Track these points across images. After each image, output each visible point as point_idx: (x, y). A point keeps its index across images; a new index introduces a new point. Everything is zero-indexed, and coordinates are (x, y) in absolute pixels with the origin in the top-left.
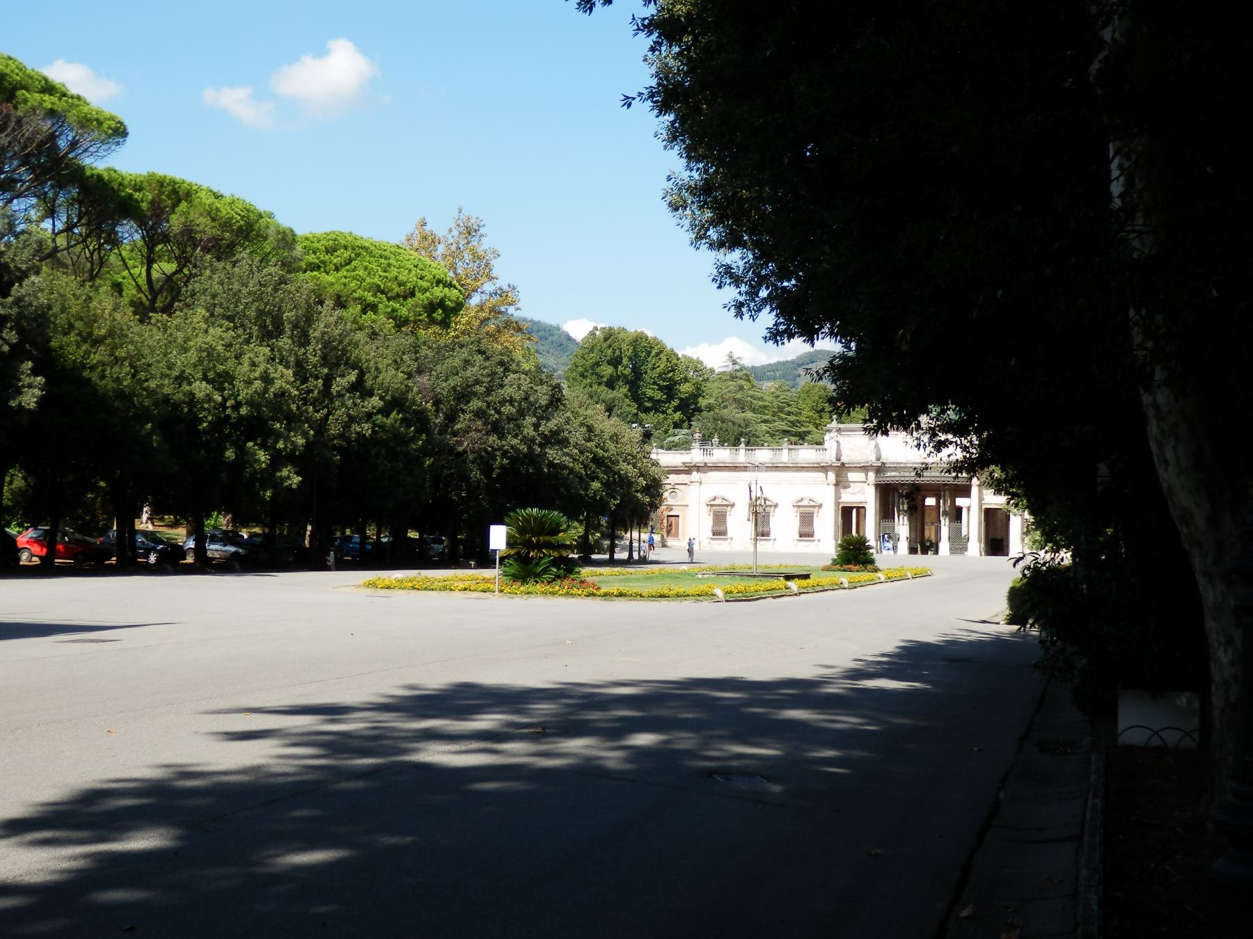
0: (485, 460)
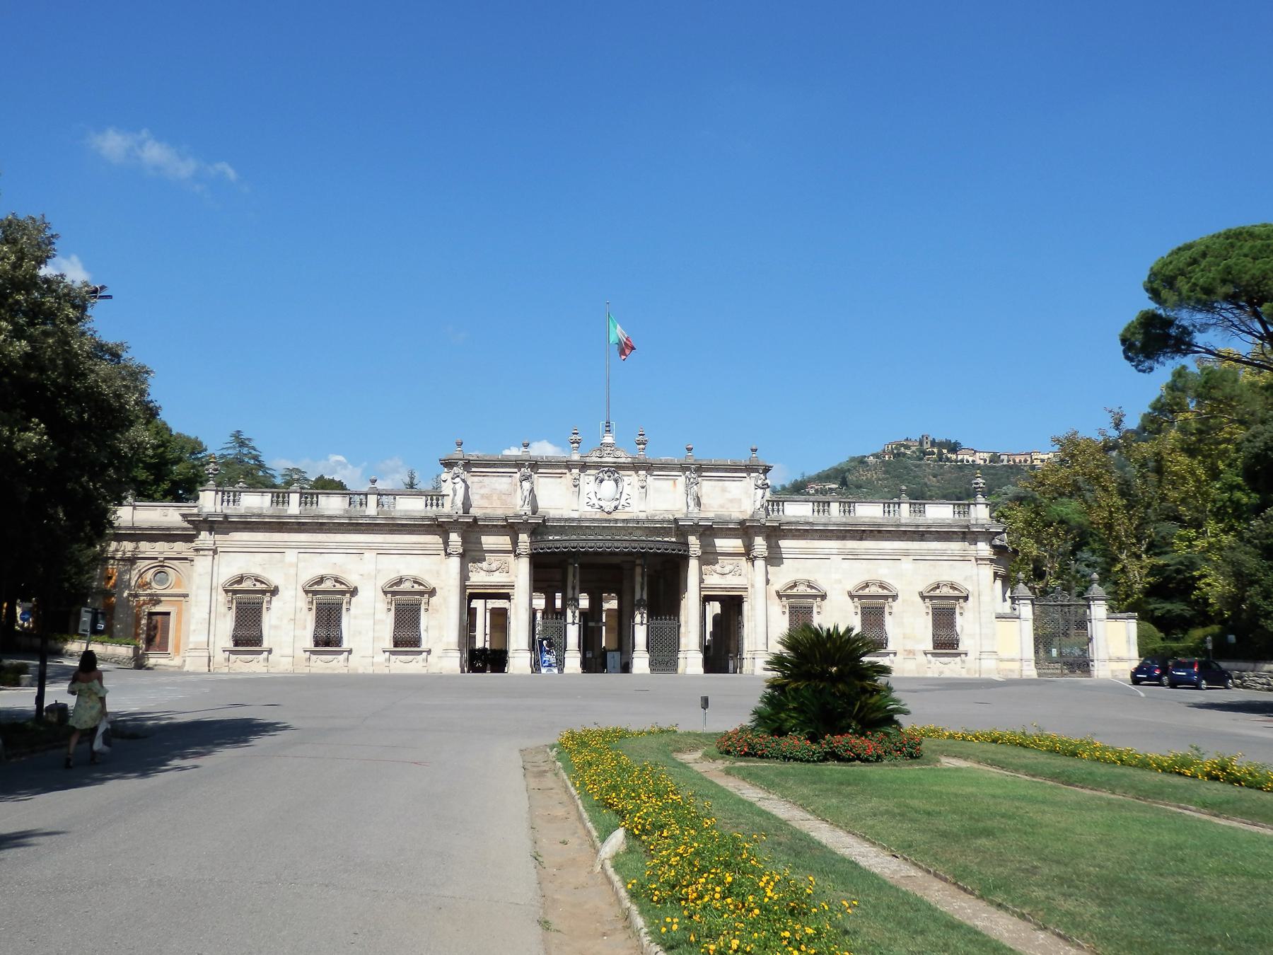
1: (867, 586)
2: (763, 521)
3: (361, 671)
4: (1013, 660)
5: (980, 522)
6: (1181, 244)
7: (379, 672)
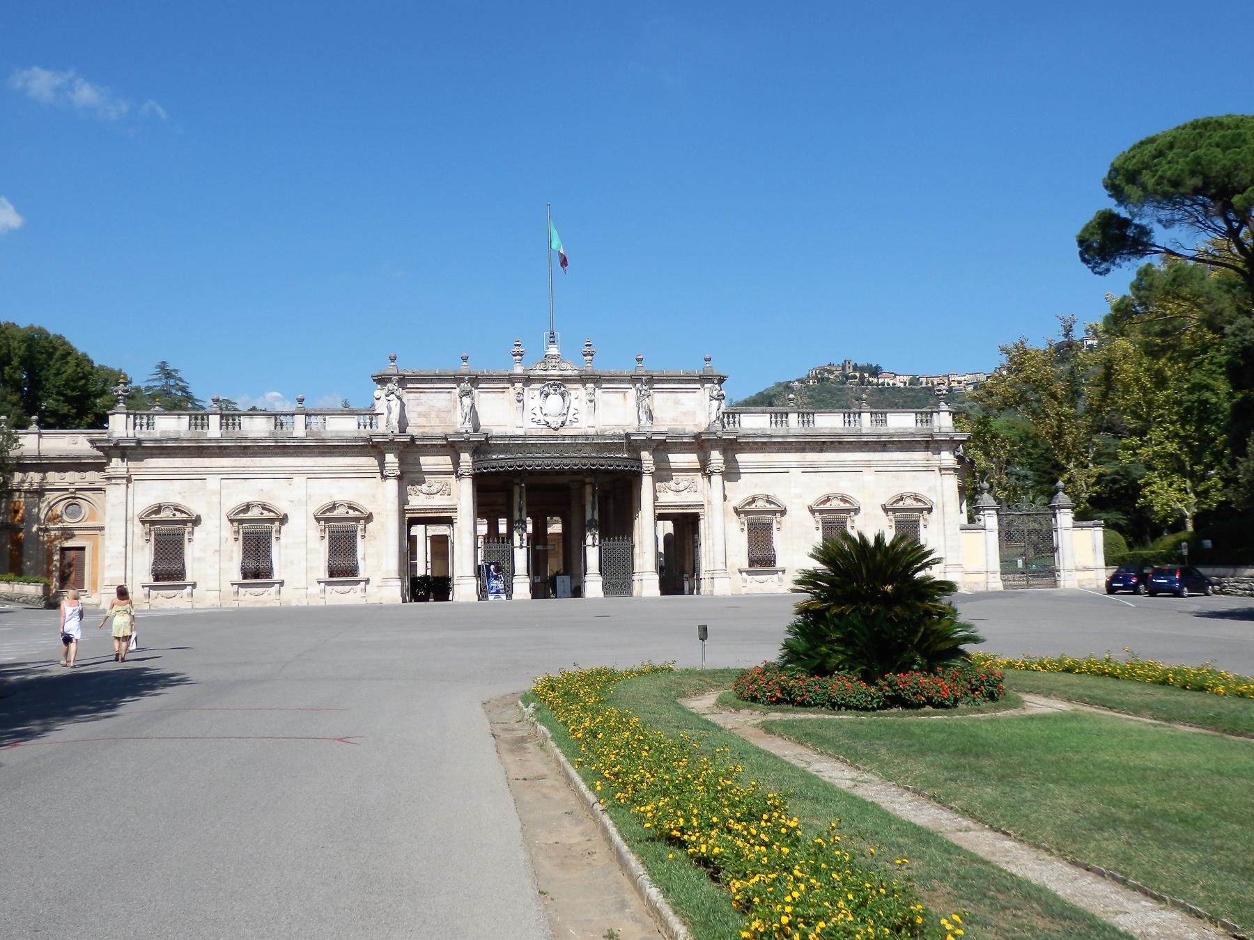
1: (828, 499)
2: (719, 434)
3: (294, 603)
4: (978, 572)
5: (944, 430)
6: (1143, 138)
7: (315, 604)
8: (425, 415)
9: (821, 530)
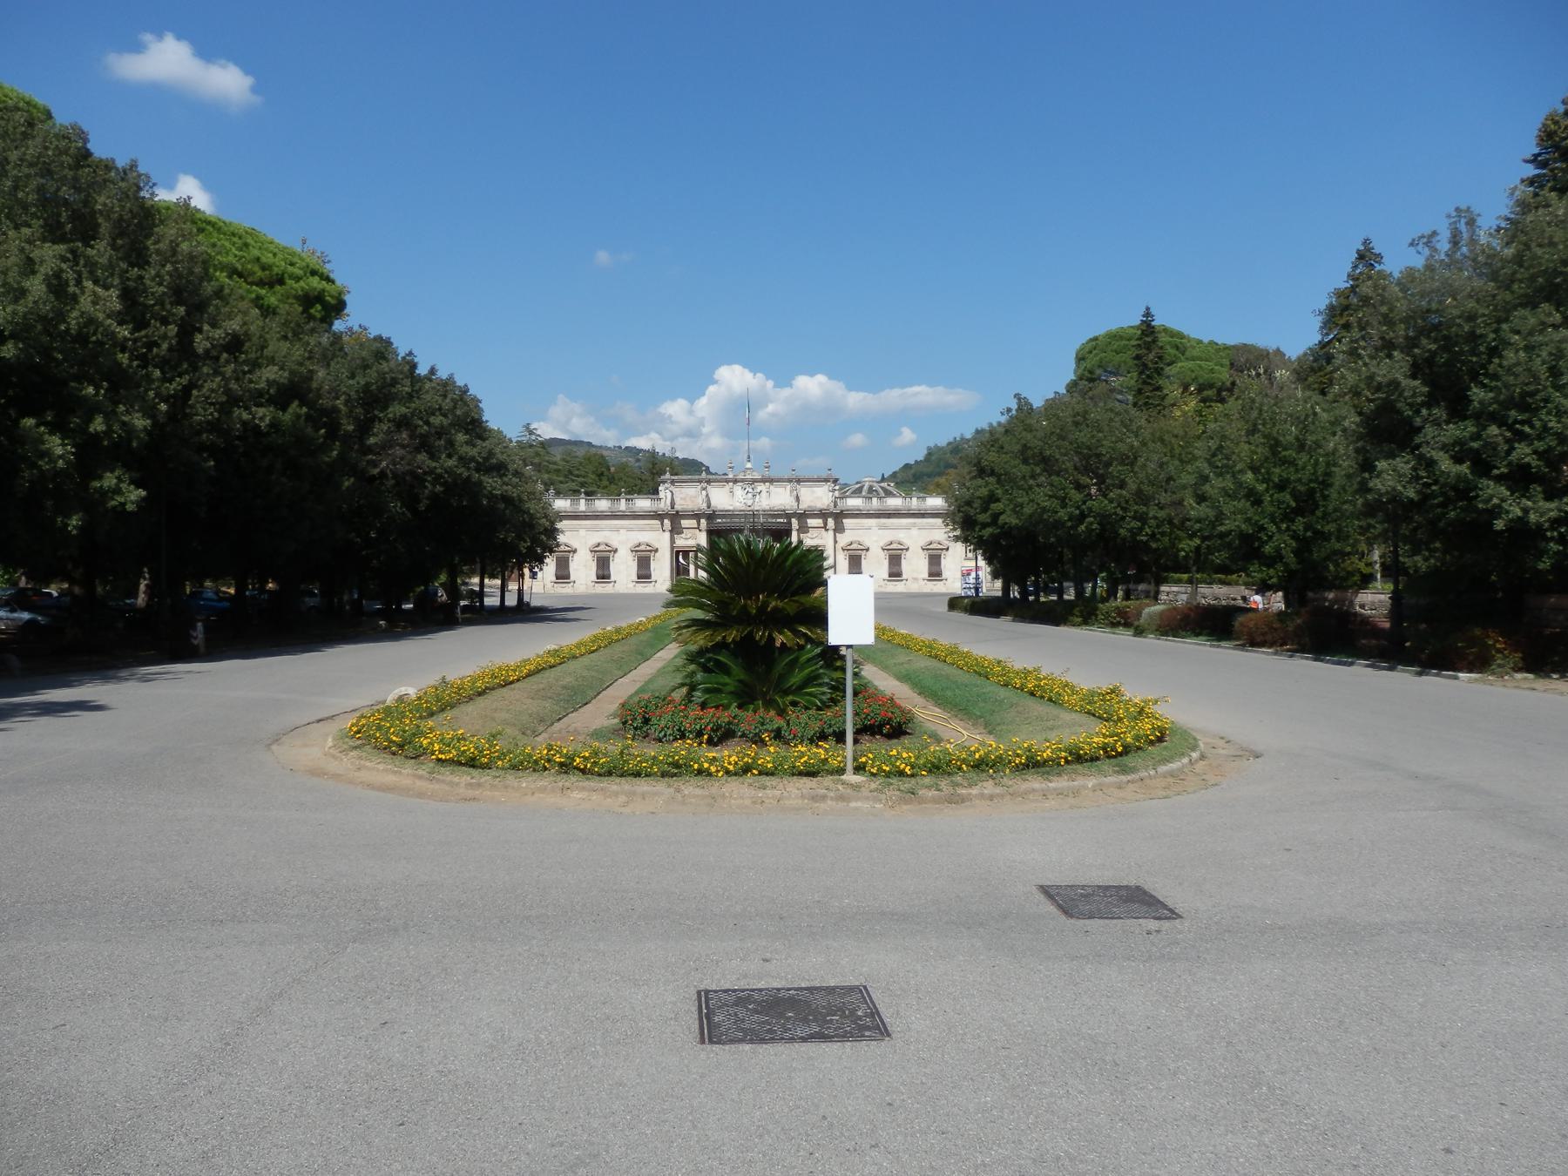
0: (408, 485)
3: (621, 592)
6: (1091, 337)
8: (684, 499)
9: (887, 560)
